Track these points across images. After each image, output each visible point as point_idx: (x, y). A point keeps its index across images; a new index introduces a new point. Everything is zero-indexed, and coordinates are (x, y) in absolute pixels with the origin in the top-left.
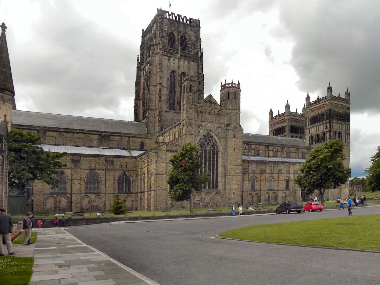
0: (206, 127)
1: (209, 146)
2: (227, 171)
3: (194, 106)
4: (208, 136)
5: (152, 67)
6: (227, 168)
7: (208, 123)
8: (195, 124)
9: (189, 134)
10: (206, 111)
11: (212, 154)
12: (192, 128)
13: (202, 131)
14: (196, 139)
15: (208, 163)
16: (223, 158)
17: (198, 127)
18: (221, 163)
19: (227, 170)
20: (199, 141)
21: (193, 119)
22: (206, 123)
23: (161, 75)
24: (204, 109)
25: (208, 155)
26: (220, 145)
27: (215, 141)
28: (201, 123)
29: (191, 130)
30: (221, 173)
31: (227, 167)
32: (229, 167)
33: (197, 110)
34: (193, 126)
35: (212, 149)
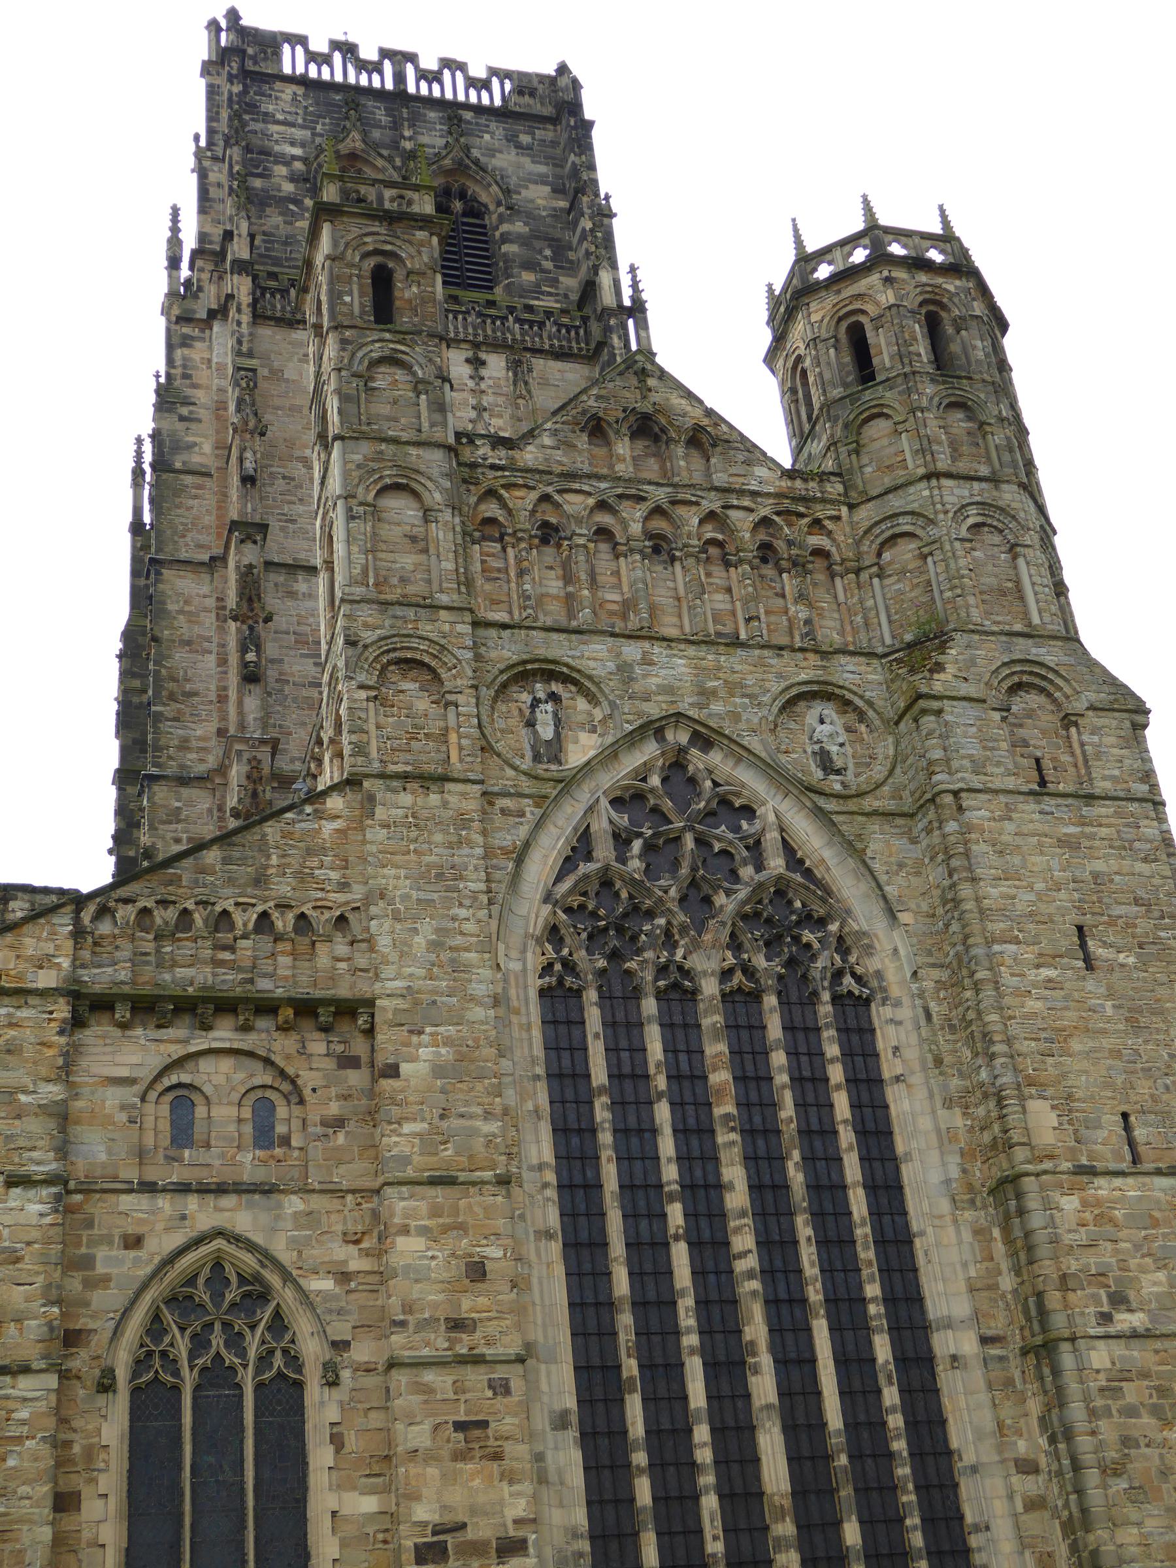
0: (637, 687)
1: (716, 933)
2: (1047, 1268)
3: (434, 461)
4: (683, 806)
5: (182, 419)
6: (1036, 1220)
7: (658, 651)
8: (478, 657)
9: (405, 777)
10: (605, 519)
11: (775, 1029)
12: (434, 710)
13: (585, 738)
14: (510, 836)
15: (734, 1173)
16: (955, 1083)
17: (526, 697)
18: (934, 1157)
19: (1043, 1251)
20: (568, 864)
21: (444, 599)
22: (632, 651)
23: (248, 454)
24: (575, 504)
25: (716, 1049)
26: (877, 908)
27: (794, 859)
28: (559, 648)
29: (435, 727)
30: (977, 1316)
31: (1033, 1202)
32: (1070, 1204)
33: (491, 509)
34: (458, 679)
35: (760, 961)
